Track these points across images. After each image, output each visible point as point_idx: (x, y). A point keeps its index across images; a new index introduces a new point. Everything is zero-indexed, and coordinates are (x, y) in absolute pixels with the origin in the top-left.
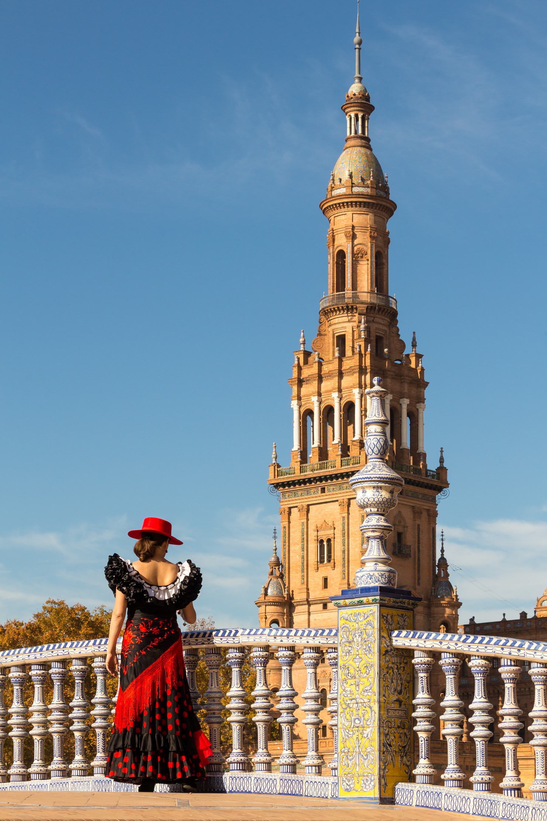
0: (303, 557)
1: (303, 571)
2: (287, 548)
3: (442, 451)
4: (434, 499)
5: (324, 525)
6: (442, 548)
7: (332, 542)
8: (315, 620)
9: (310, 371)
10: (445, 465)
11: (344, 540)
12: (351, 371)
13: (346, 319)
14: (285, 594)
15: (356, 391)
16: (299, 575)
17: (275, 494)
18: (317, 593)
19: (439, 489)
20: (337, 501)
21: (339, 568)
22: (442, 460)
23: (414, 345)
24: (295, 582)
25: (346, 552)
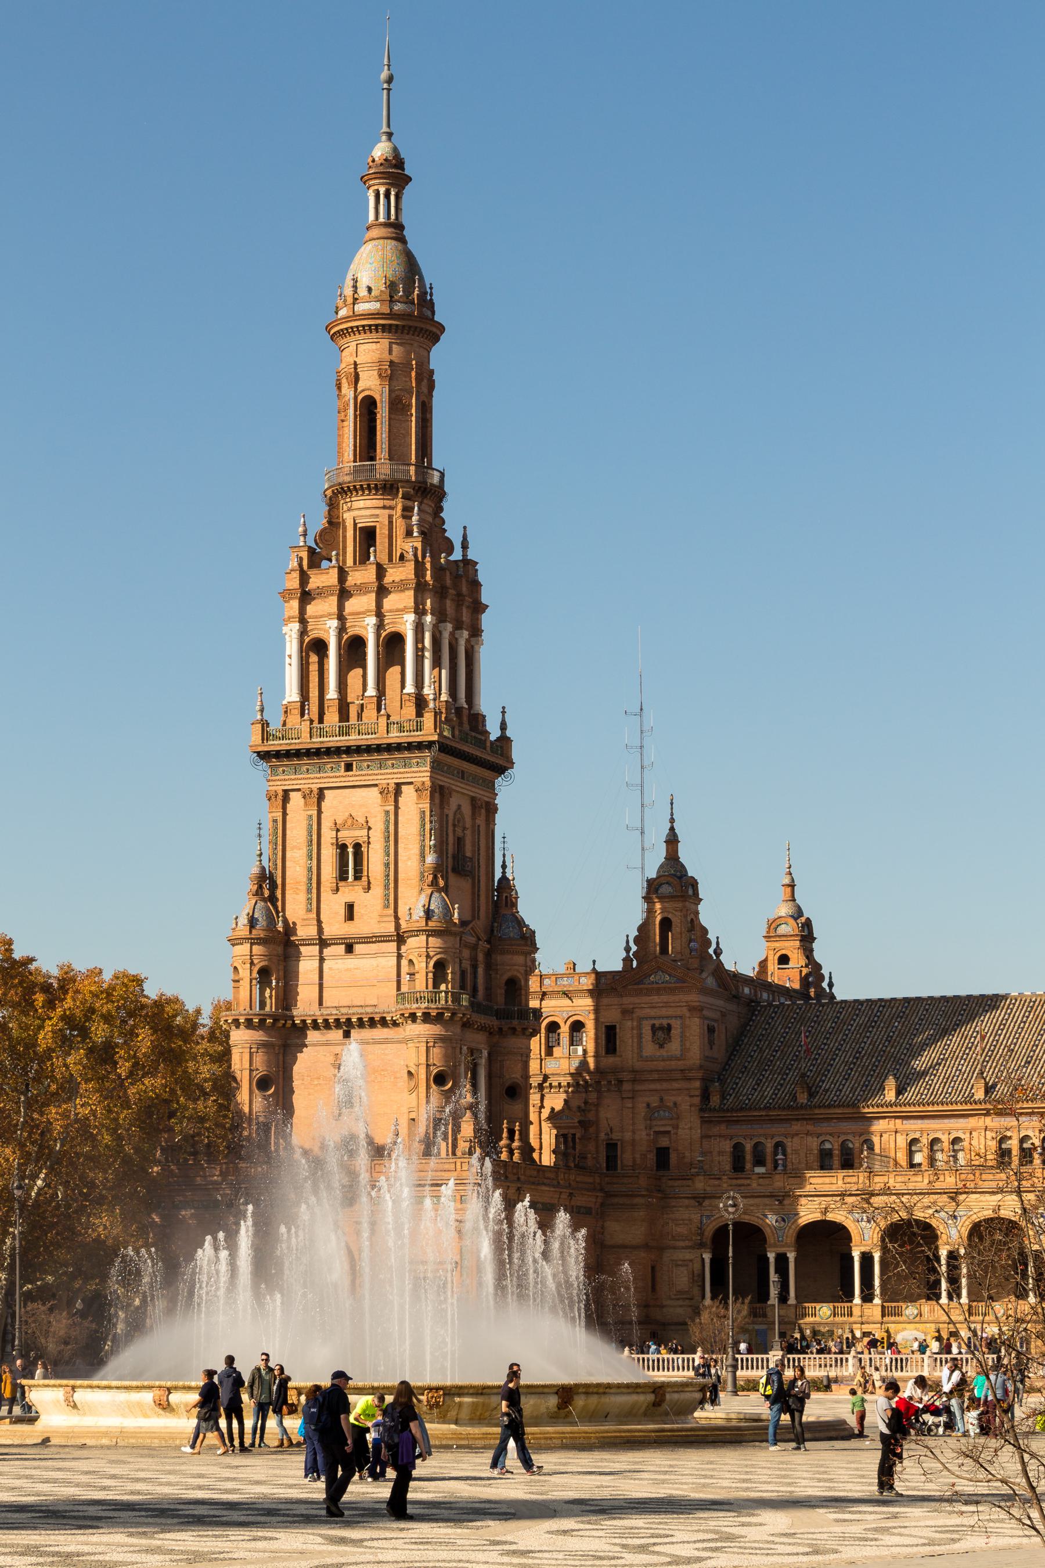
0: (310, 869)
1: (309, 891)
2: (280, 854)
3: (503, 712)
4: (491, 787)
5: (350, 822)
6: (504, 862)
7: (364, 849)
8: (330, 969)
9: (324, 578)
10: (508, 733)
11: (387, 847)
12: (401, 586)
13: (381, 503)
14: (280, 927)
15: (410, 618)
16: (302, 897)
17: (260, 768)
18: (335, 926)
19: (501, 769)
20: (376, 785)
21: (377, 890)
22: (503, 726)
23: (465, 546)
24: (295, 907)
25: (392, 866)
